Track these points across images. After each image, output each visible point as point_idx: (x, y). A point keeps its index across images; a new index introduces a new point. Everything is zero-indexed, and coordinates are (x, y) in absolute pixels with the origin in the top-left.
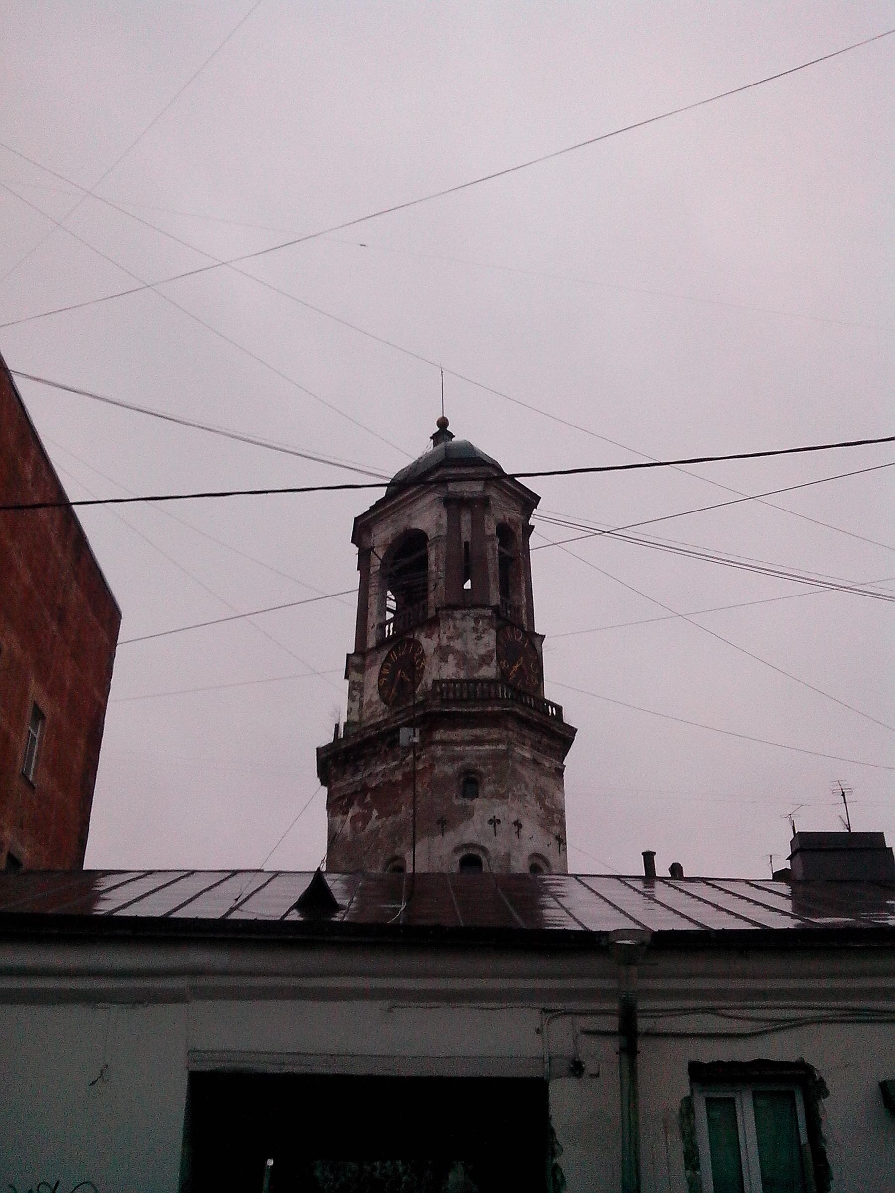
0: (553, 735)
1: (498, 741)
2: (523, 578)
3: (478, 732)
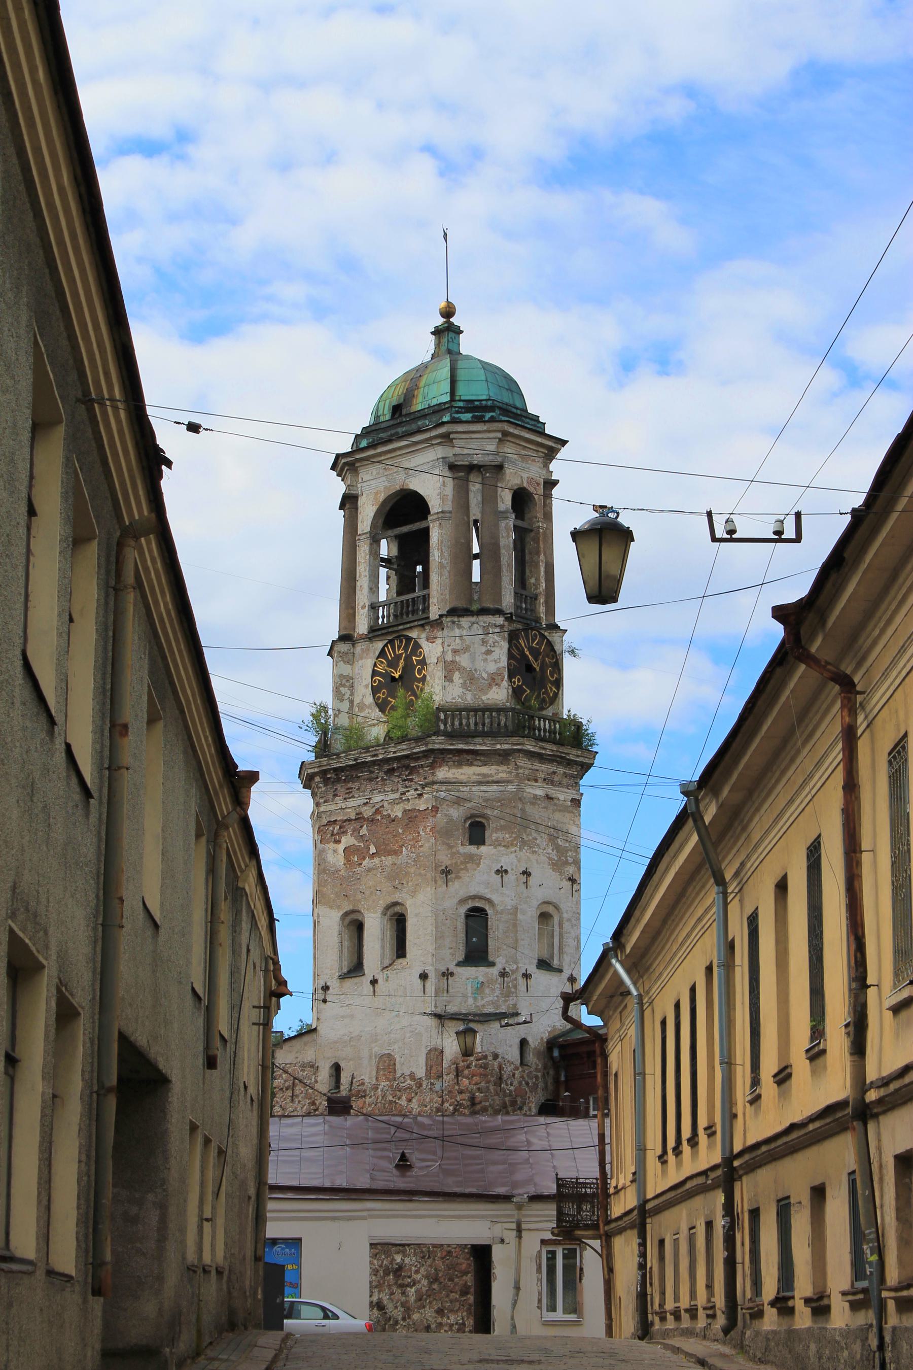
0: (570, 763)
2: (542, 557)
3: (485, 770)
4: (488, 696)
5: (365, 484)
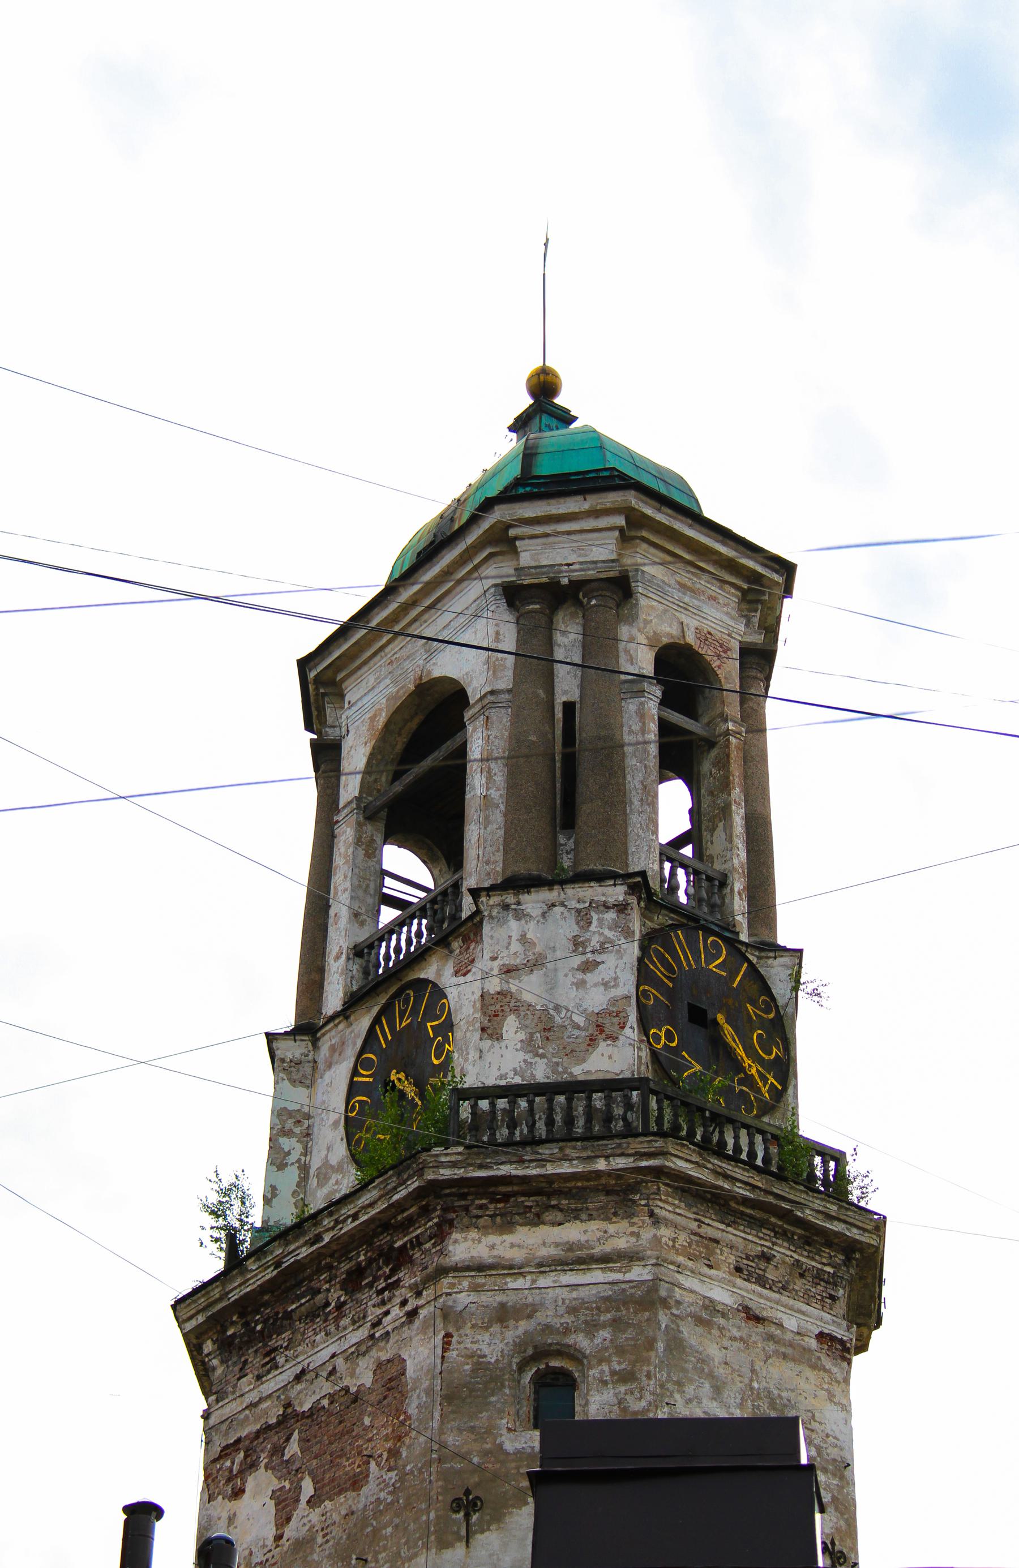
1: (631, 1257)
3: (573, 1232)
4: (586, 1066)
5: (354, 709)
